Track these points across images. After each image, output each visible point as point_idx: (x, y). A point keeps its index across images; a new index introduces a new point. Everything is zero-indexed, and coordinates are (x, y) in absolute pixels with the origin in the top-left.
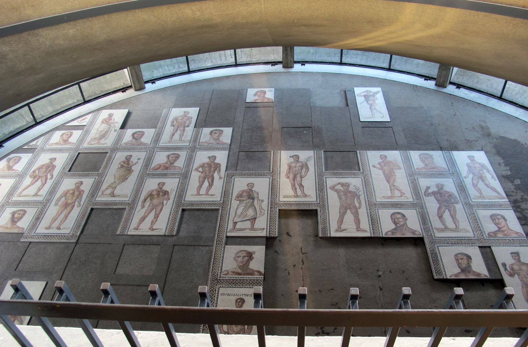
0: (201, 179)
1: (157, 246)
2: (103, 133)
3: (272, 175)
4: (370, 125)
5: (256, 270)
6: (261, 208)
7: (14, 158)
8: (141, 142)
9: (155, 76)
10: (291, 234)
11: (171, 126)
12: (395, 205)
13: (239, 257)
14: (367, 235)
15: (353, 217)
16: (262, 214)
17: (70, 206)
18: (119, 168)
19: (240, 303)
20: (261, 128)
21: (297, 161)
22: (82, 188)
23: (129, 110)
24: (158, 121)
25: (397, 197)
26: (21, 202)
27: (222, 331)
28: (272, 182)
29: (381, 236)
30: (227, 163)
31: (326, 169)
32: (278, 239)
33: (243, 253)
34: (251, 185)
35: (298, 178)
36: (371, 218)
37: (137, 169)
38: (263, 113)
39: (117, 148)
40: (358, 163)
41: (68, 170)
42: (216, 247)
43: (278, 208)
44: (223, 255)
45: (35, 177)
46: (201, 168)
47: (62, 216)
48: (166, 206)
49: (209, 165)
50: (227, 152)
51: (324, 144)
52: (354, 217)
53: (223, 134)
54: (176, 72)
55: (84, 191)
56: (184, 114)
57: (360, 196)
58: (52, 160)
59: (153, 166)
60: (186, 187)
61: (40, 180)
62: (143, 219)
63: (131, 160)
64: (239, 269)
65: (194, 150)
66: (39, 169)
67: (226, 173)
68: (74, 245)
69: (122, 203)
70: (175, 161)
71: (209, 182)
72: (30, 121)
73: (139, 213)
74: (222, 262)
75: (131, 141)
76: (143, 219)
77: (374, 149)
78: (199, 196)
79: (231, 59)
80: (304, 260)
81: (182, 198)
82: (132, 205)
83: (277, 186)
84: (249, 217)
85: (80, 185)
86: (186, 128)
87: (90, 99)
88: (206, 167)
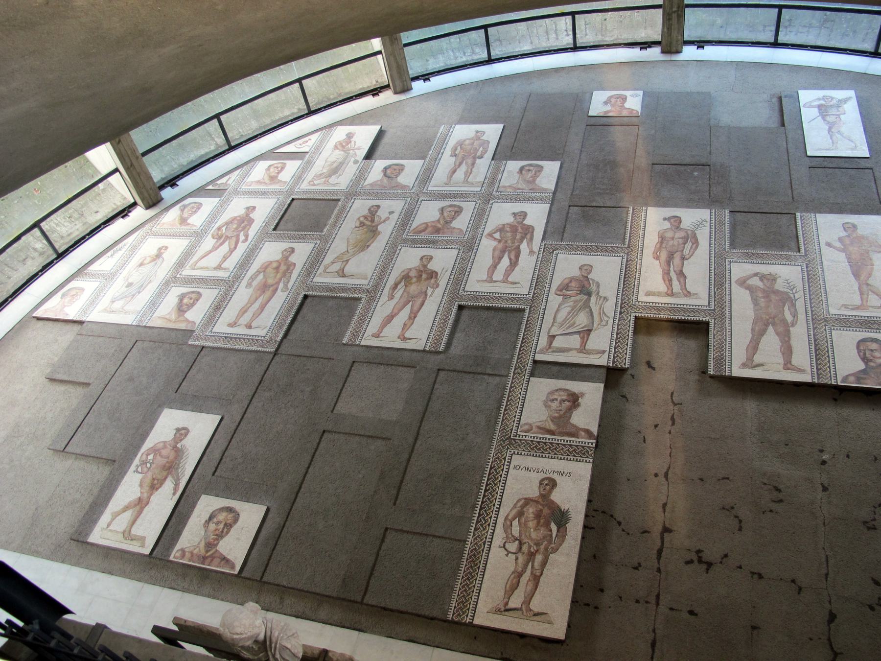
0: (497, 253)
1: (409, 369)
2: (335, 165)
3: (628, 253)
4: (826, 164)
5: (583, 427)
6: (602, 313)
7: (191, 205)
8: (397, 182)
9: (430, 69)
10: (655, 365)
11: (451, 156)
12: (866, 324)
13: (553, 400)
14: (806, 378)
15: (778, 341)
16: (604, 323)
17: (271, 288)
18: (356, 227)
19: (548, 487)
20: (613, 165)
21: (678, 228)
22: (293, 259)
23: (381, 127)
24: (430, 148)
25: (872, 307)
26: (195, 279)
27: (510, 536)
28: (626, 265)
29: (833, 383)
30: (546, 226)
31: (733, 245)
32: (629, 372)
33: (562, 393)
34: (587, 269)
35: (677, 260)
36: (816, 345)
37: (386, 230)
38: (619, 137)
39: (356, 192)
40: (797, 237)
41: (273, 227)
42: (513, 378)
43: (634, 314)
44: (526, 395)
45: (220, 238)
47: (257, 305)
48: (430, 298)
49: (514, 229)
50: (547, 206)
51: (731, 196)
52: (781, 342)
53: (543, 174)
54: (467, 61)
55: (295, 264)
56: (476, 136)
57: (796, 300)
58: (250, 210)
59: (414, 225)
60: (469, 265)
61: (227, 243)
62: (390, 318)
63: (377, 214)
64: (550, 423)
65: (489, 200)
66: (227, 224)
67: (544, 243)
68: (271, 356)
69: (355, 289)
70: (453, 218)
71: (510, 259)
72: (221, 145)
73: (383, 307)
74: (522, 408)
75: (380, 180)
76: (390, 318)
77: (831, 211)
78: (492, 284)
79: (567, 38)
80: (675, 417)
81: (461, 285)
82: (373, 293)
83: (636, 272)
84: (578, 327)
85: (290, 255)
86: (478, 161)
87: (319, 107)
88: (508, 232)
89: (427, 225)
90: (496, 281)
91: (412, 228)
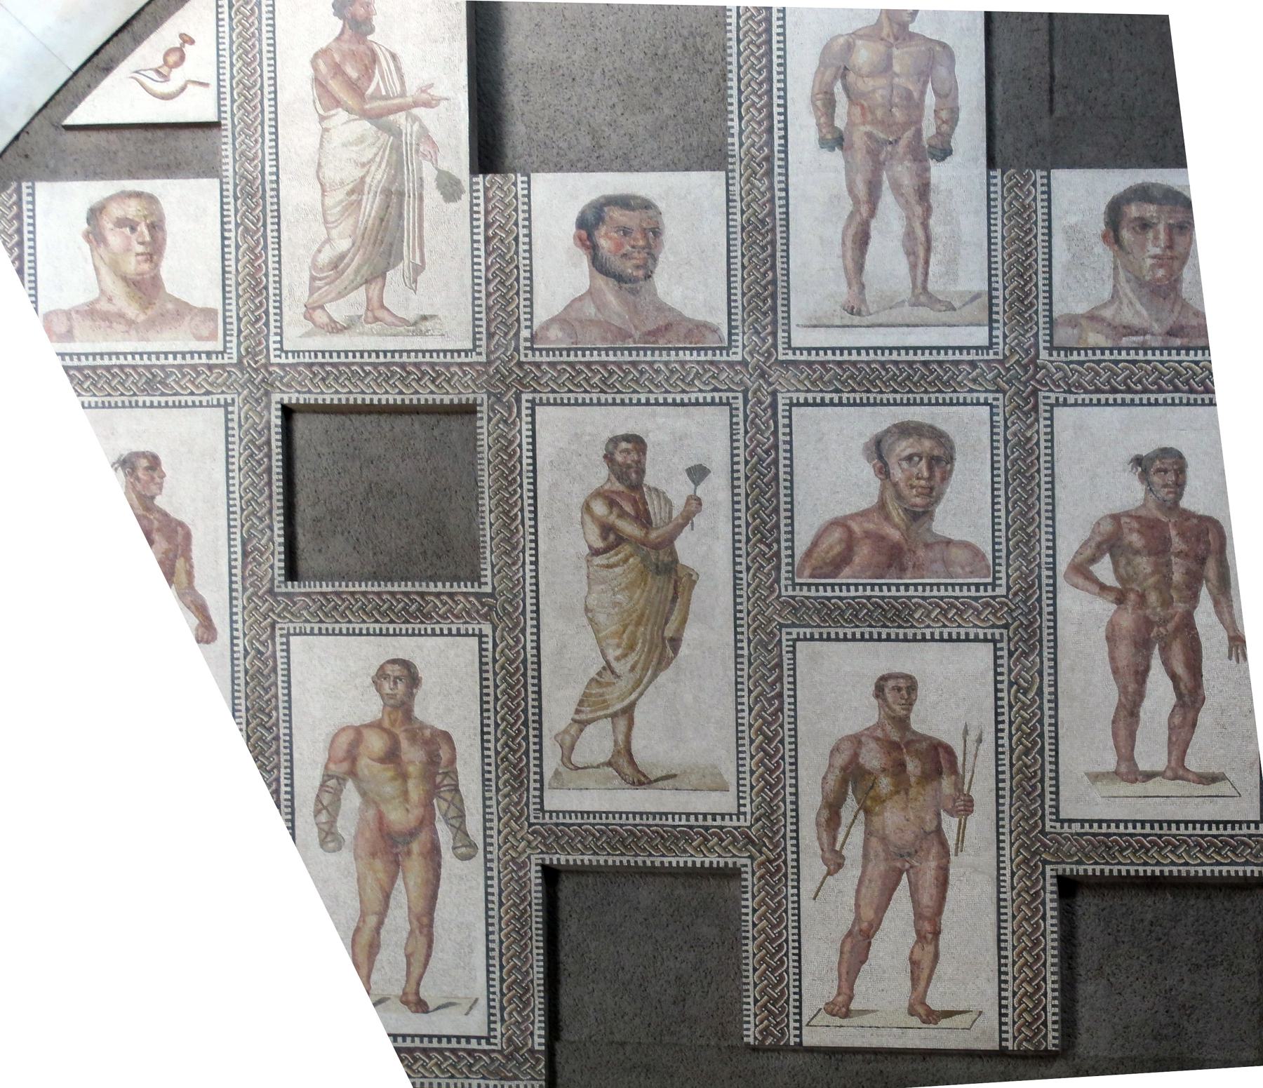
0: (1125, 651)
17: (415, 847)
18: (596, 553)
46: (1107, 560)
59: (803, 541)
71: (1174, 677)
75: (590, 292)
78: (1139, 788)
88: (1137, 552)
89: (850, 531)
90: (1149, 776)
91: (800, 549)
